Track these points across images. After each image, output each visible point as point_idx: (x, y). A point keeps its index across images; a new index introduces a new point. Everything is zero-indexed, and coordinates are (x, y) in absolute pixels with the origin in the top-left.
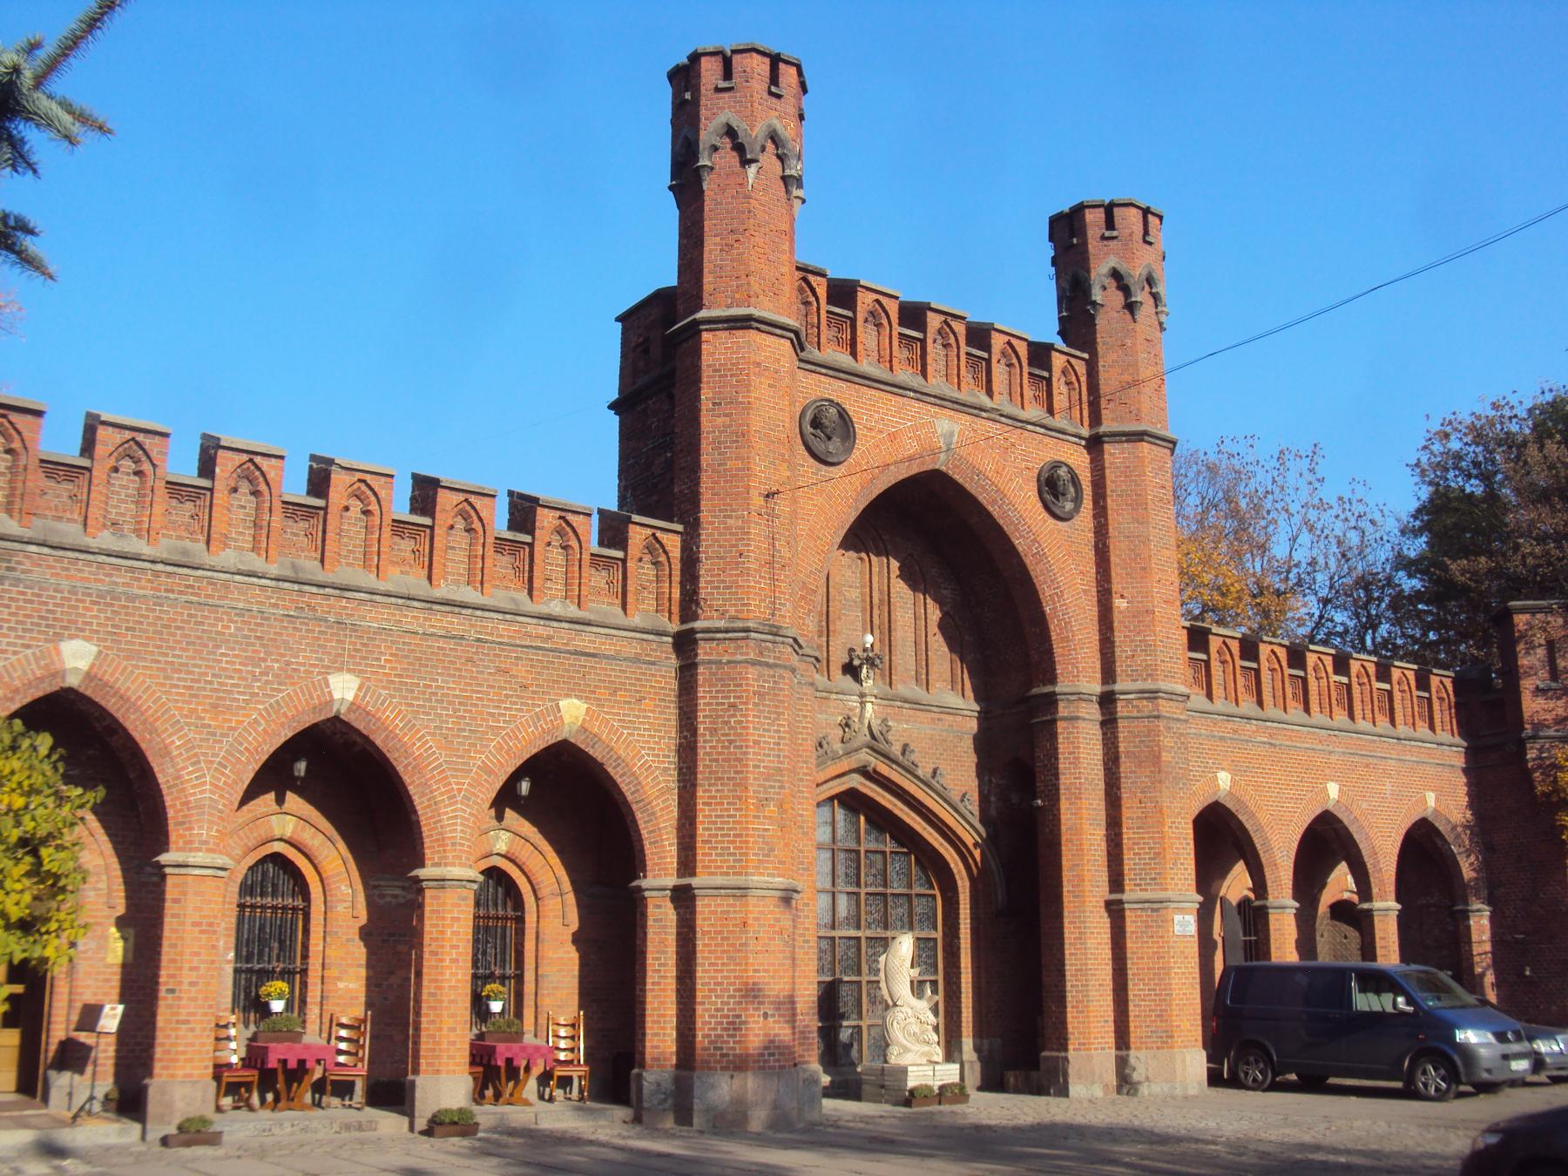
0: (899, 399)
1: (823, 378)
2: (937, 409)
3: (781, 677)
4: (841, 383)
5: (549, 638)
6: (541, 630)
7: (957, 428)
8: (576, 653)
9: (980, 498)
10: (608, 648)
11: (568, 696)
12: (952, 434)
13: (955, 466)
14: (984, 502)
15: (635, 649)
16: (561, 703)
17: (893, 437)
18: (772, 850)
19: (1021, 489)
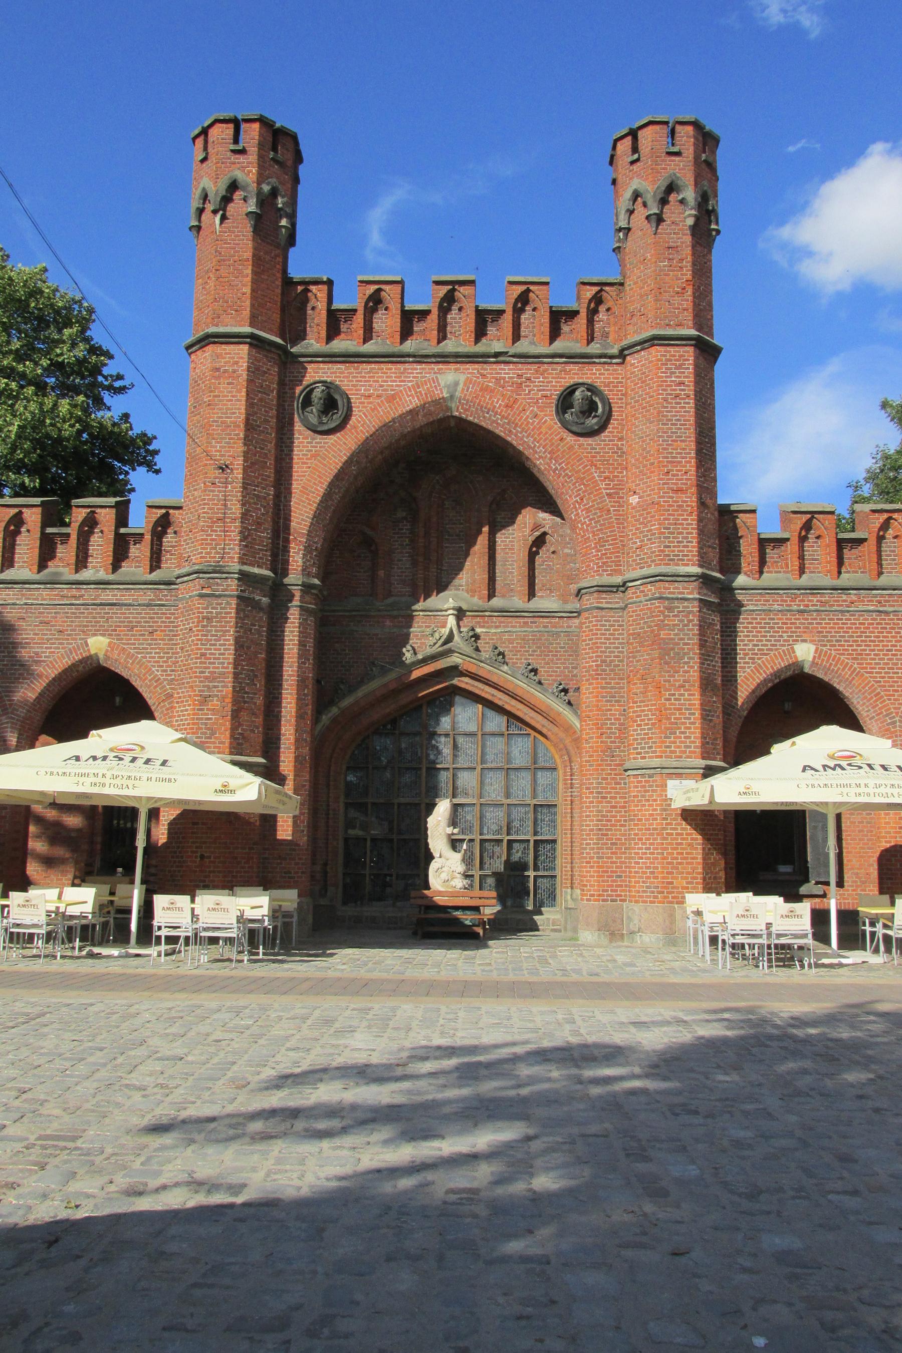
0: (399, 366)
1: (322, 365)
2: (441, 366)
3: (228, 603)
4: (339, 366)
5: (82, 596)
6: (74, 592)
7: (462, 378)
8: (101, 604)
9: (497, 431)
10: (127, 598)
11: (95, 635)
12: (456, 384)
13: (466, 410)
14: (502, 434)
15: (144, 600)
16: (89, 641)
17: (391, 399)
18: (213, 734)
19: (536, 416)
